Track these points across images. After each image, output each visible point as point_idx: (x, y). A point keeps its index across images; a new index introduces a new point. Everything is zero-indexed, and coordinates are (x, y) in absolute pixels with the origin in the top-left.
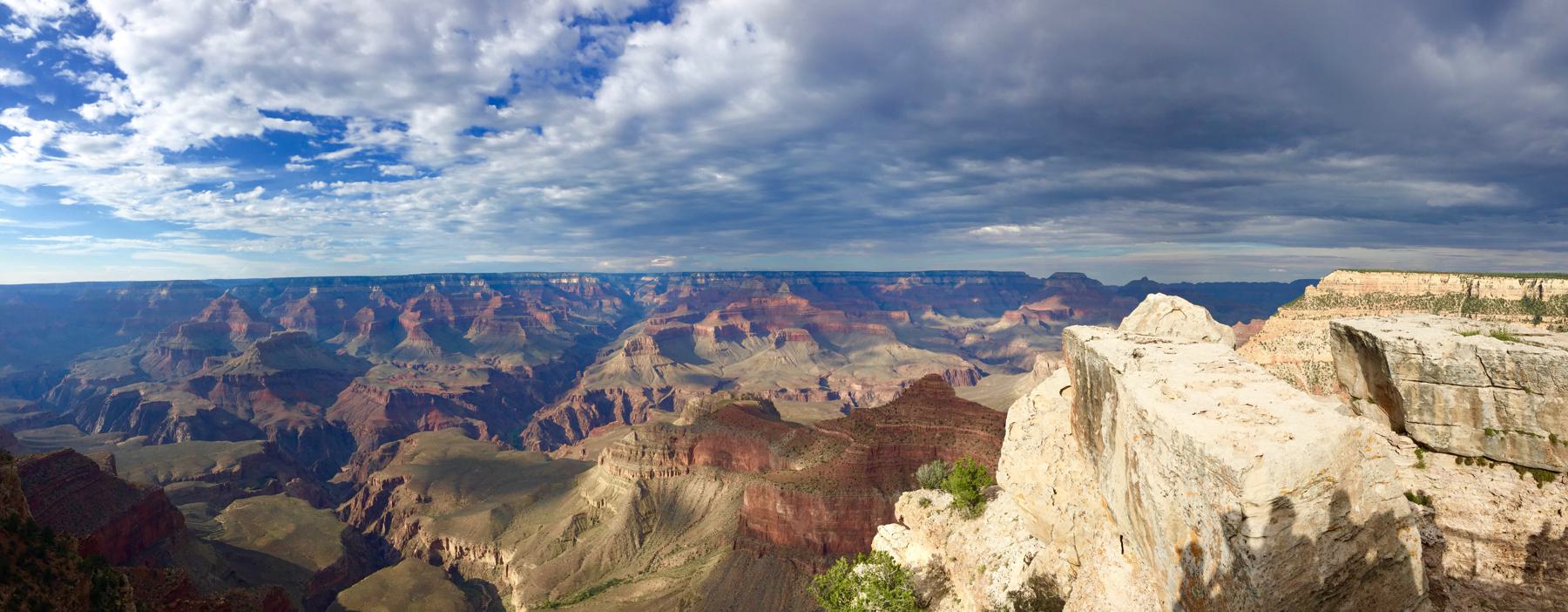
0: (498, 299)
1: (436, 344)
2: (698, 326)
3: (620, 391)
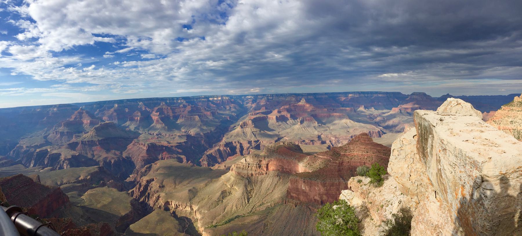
0: (189, 107)
1: (166, 125)
2: (269, 116)
3: (238, 142)
